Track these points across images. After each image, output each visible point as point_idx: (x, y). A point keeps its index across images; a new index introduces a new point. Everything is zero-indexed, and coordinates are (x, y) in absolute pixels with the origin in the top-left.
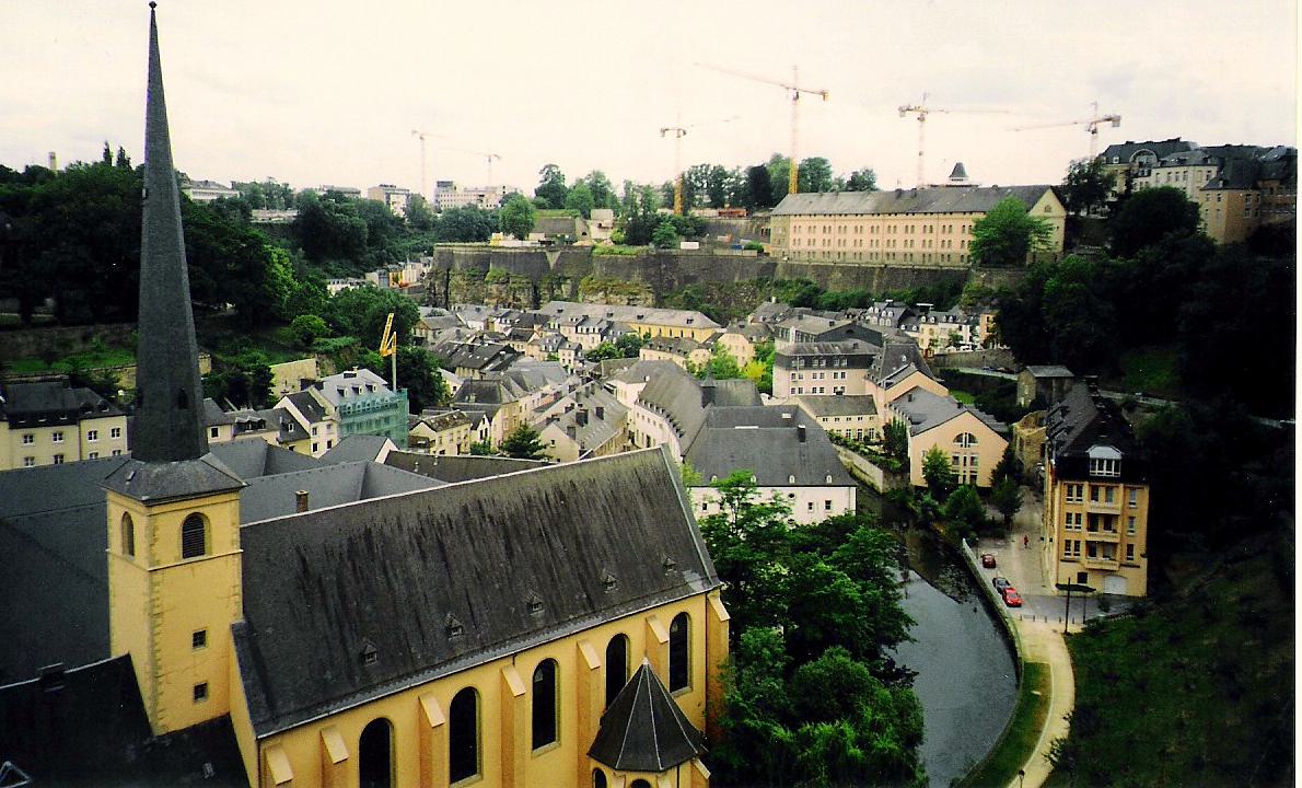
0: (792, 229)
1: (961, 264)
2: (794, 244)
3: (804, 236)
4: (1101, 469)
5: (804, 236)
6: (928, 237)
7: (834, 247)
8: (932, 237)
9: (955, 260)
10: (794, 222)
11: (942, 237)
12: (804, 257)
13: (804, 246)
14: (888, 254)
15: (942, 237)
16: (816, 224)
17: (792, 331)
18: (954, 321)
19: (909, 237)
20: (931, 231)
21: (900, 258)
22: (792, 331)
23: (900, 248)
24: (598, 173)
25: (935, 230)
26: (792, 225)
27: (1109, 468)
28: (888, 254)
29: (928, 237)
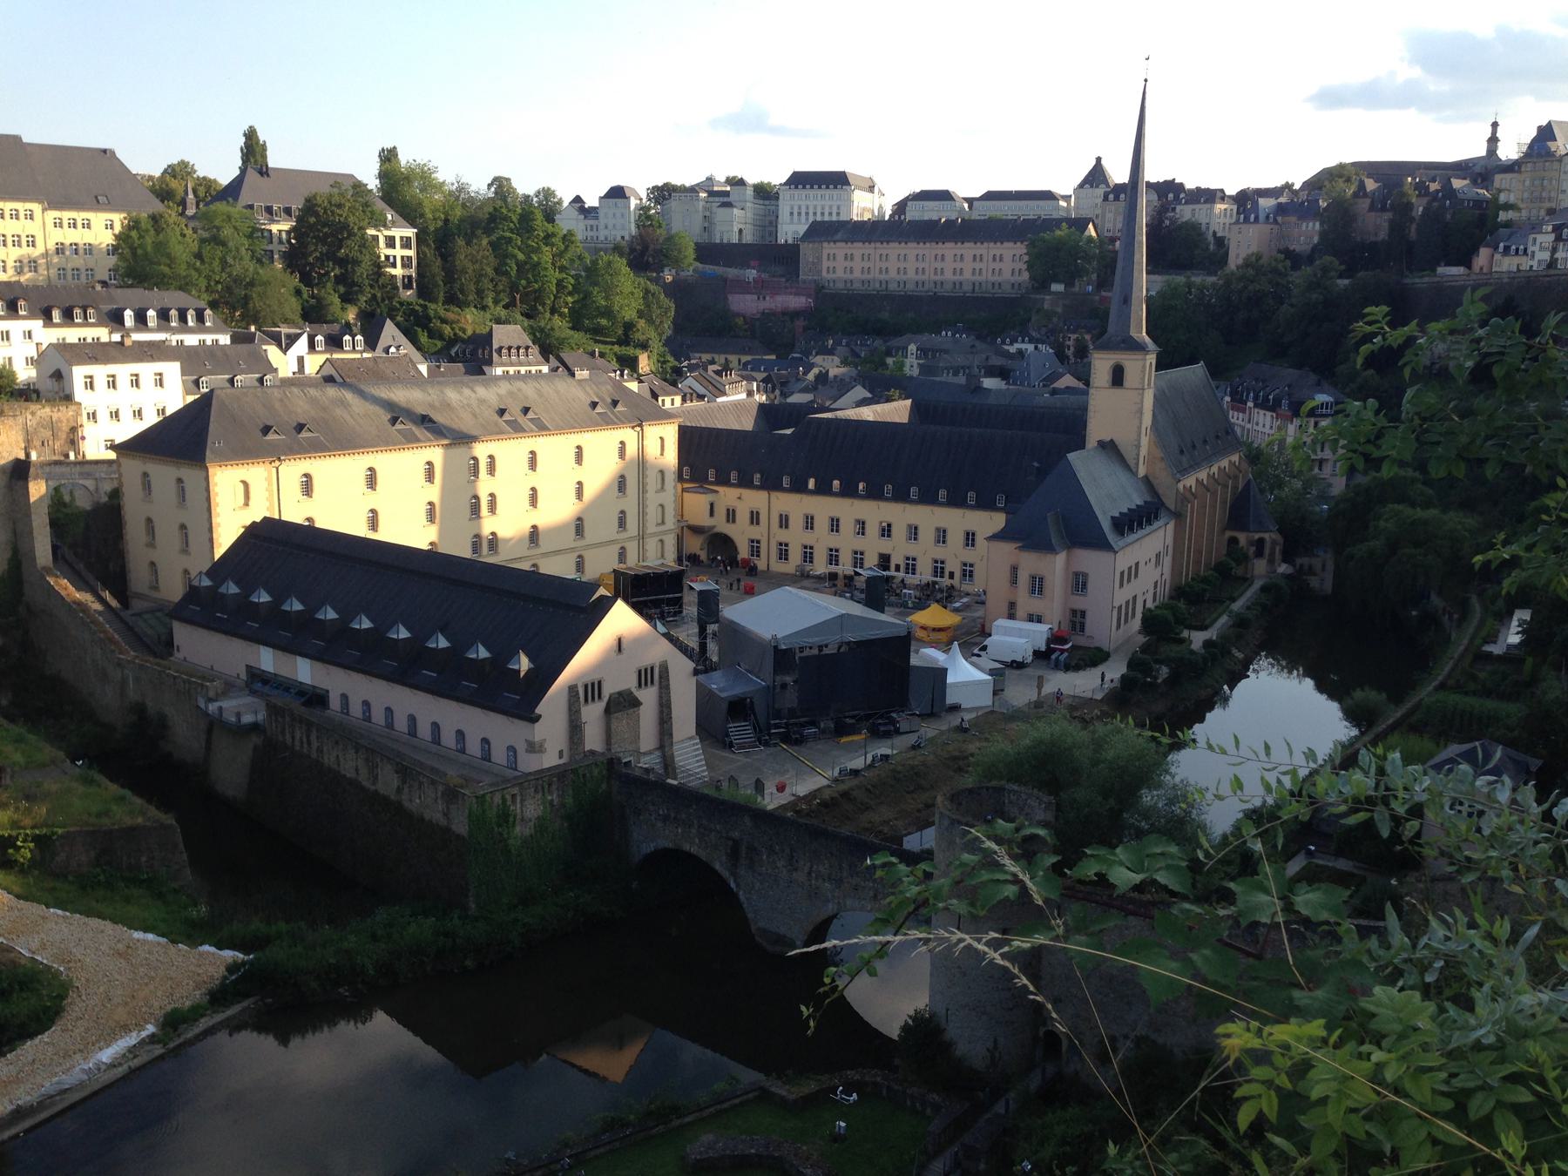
0: (825, 257)
1: (1014, 291)
2: (828, 272)
3: (840, 264)
4: (1327, 408)
5: (840, 264)
6: (978, 266)
7: (875, 274)
8: (983, 266)
9: (1007, 288)
10: (828, 248)
11: (992, 265)
12: (840, 285)
13: (840, 274)
14: (935, 283)
15: (992, 265)
16: (854, 252)
17: (912, 348)
18: (1030, 342)
19: (959, 265)
20: (981, 260)
21: (948, 287)
22: (912, 348)
23: (949, 275)
24: (549, 189)
25: (985, 259)
26: (825, 252)
27: (1327, 408)
28: (935, 283)
29: (978, 266)
